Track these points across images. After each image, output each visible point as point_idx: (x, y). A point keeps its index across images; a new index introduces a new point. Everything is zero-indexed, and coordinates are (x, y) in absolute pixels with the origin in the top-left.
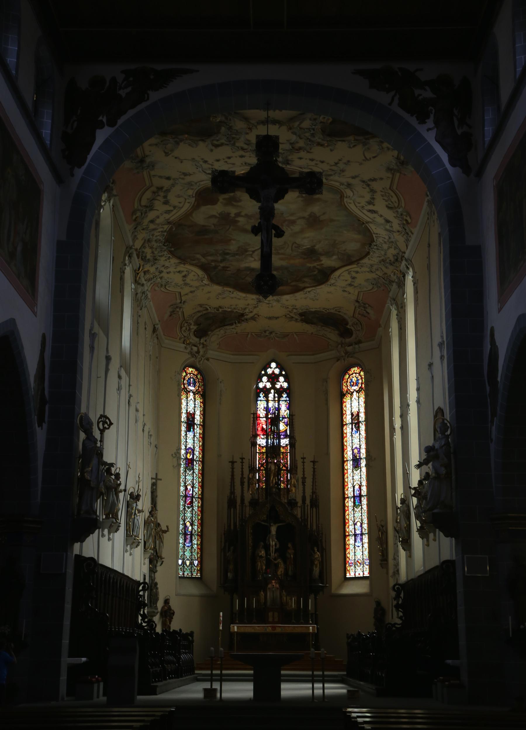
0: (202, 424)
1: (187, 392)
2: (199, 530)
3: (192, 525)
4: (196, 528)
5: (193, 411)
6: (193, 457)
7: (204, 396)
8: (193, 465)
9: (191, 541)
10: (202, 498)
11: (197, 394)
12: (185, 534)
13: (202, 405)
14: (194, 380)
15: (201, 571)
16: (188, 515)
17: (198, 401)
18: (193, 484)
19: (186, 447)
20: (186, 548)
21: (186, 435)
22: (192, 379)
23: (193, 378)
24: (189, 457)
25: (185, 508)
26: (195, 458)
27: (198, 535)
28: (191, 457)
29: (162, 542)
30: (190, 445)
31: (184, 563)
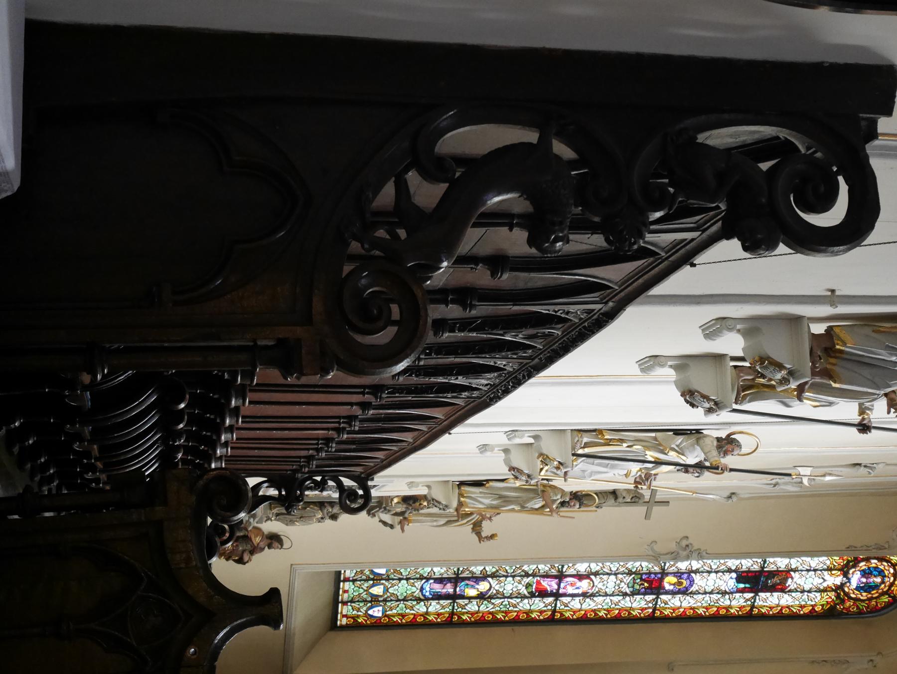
0: (756, 611)
1: (845, 571)
2: (464, 617)
3: (481, 597)
4: (473, 607)
5: (792, 587)
6: (667, 593)
7: (830, 613)
8: (645, 594)
9: (438, 597)
10: (554, 620)
11: (838, 596)
12: (456, 580)
13: (806, 610)
14: (876, 587)
15: (355, 626)
16: (509, 586)
17: (819, 601)
18: (593, 595)
19: (696, 572)
20: (418, 584)
21: (730, 571)
22: (878, 580)
23: (883, 582)
24: (669, 582)
25: (527, 575)
26: (663, 597)
27: (452, 614)
28: (668, 587)
29: (448, 523)
30: (700, 582)
31: (377, 579)
